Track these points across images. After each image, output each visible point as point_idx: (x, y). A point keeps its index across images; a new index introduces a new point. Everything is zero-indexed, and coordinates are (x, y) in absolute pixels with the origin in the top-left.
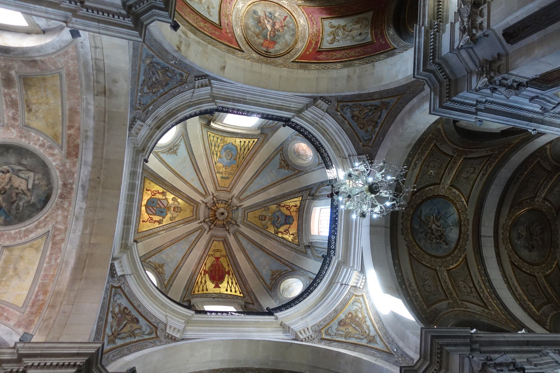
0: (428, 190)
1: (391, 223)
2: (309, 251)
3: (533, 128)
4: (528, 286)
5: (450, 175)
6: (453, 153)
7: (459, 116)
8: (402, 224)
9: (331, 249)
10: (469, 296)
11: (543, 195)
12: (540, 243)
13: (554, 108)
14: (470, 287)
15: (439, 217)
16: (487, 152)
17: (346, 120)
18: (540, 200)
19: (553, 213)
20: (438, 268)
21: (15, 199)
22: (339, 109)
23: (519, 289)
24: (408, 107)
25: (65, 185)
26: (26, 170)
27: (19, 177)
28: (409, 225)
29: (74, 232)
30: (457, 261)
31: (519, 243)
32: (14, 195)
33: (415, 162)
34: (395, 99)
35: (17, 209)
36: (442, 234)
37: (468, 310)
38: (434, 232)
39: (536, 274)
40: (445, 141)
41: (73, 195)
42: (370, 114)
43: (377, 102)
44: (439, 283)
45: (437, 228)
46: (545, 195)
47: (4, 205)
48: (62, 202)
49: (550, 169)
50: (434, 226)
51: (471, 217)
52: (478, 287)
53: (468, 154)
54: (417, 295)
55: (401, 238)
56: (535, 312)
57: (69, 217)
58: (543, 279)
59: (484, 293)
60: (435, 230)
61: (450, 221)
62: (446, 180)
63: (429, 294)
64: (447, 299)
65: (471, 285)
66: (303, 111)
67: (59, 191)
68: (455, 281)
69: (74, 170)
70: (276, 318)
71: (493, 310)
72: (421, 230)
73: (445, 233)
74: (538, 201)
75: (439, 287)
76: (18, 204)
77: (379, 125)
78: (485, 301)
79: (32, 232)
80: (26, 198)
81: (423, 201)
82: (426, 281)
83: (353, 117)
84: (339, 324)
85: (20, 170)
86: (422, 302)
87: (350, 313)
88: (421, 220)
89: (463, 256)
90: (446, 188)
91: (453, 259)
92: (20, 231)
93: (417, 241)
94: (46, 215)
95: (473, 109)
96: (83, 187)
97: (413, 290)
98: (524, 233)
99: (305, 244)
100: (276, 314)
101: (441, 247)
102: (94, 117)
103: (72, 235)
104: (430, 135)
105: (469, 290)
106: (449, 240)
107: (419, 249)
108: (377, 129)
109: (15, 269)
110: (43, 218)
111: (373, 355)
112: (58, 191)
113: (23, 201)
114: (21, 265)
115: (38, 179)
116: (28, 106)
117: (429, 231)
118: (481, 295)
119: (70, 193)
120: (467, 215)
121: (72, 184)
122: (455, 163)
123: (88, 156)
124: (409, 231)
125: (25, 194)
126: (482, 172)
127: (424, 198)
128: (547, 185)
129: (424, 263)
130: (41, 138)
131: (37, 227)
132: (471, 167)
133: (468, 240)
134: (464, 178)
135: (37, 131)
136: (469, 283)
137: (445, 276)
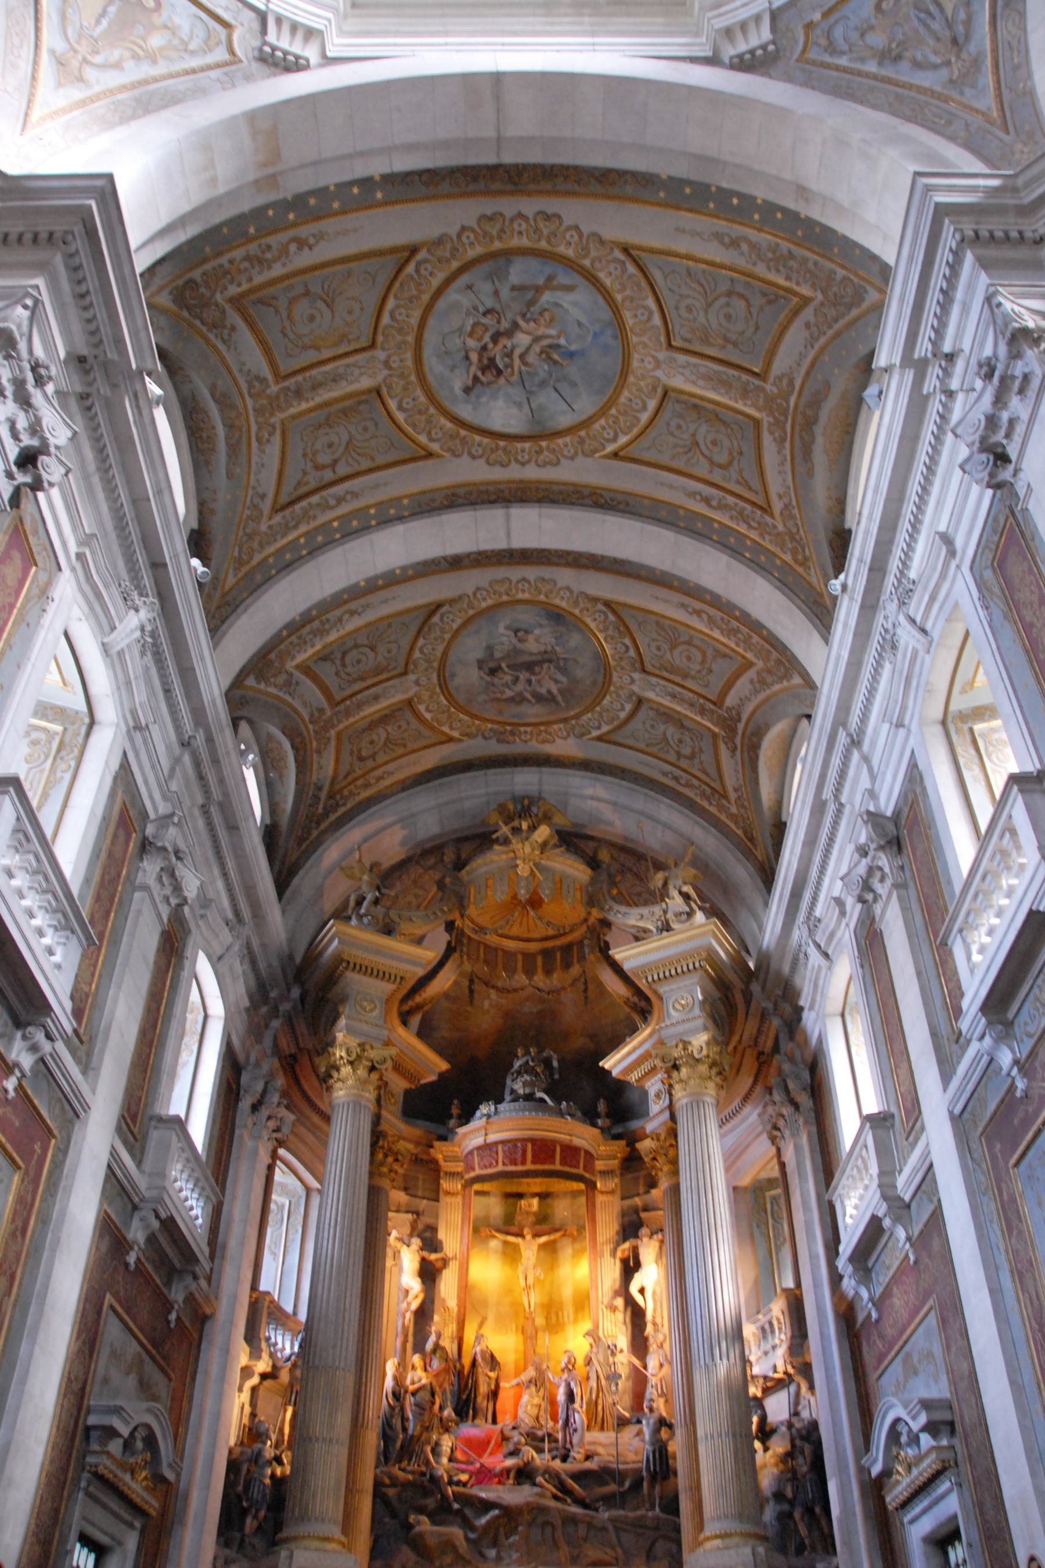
0: (646, 308)
1: (517, 166)
3: (850, 582)
4: (373, 648)
5: (701, 383)
6: (780, 378)
7: (902, 300)
8: (520, 215)
10: (305, 455)
11: (650, 695)
12: (509, 693)
13: (913, 621)
14: (335, 462)
15: (555, 357)
16: (780, 497)
18: (635, 688)
19: (599, 728)
20: (381, 355)
23: (356, 622)
28: (516, 242)
30: (414, 426)
31: (501, 629)
33: (745, 239)
36: (499, 372)
37: (254, 444)
38: (504, 341)
39: (412, 677)
40: (817, 339)
44: (326, 354)
45: (517, 352)
46: (649, 700)
49: (730, 700)
50: (522, 339)
52: (339, 489)
53: (771, 433)
54: (270, 267)
56: (293, 658)
58: (400, 697)
59: (325, 507)
60: (509, 345)
61: (546, 398)
62: (687, 372)
63: (285, 314)
65: (342, 470)
68: (344, 412)
71: (270, 527)
72: (505, 293)
73: (502, 381)
74: (633, 681)
75: (312, 356)
78: (297, 507)
81: (605, 294)
82: (328, 305)
86: (250, 279)
88: (538, 290)
89: (435, 447)
90: (659, 373)
91: (420, 412)
93: (464, 279)
95: (923, 348)
97: (284, 251)
98: (532, 646)
101: (453, 368)
104: (841, 273)
105: (324, 459)
106: (484, 399)
107: (436, 282)
117: (505, 325)
118: (315, 499)
120: (572, 458)
122: (745, 393)
124: (497, 245)
126: (714, 492)
127: (619, 297)
128: (682, 701)
129: (391, 303)
132: (730, 454)
133: (488, 463)
134: (694, 435)
136: (348, 463)
137: (357, 381)
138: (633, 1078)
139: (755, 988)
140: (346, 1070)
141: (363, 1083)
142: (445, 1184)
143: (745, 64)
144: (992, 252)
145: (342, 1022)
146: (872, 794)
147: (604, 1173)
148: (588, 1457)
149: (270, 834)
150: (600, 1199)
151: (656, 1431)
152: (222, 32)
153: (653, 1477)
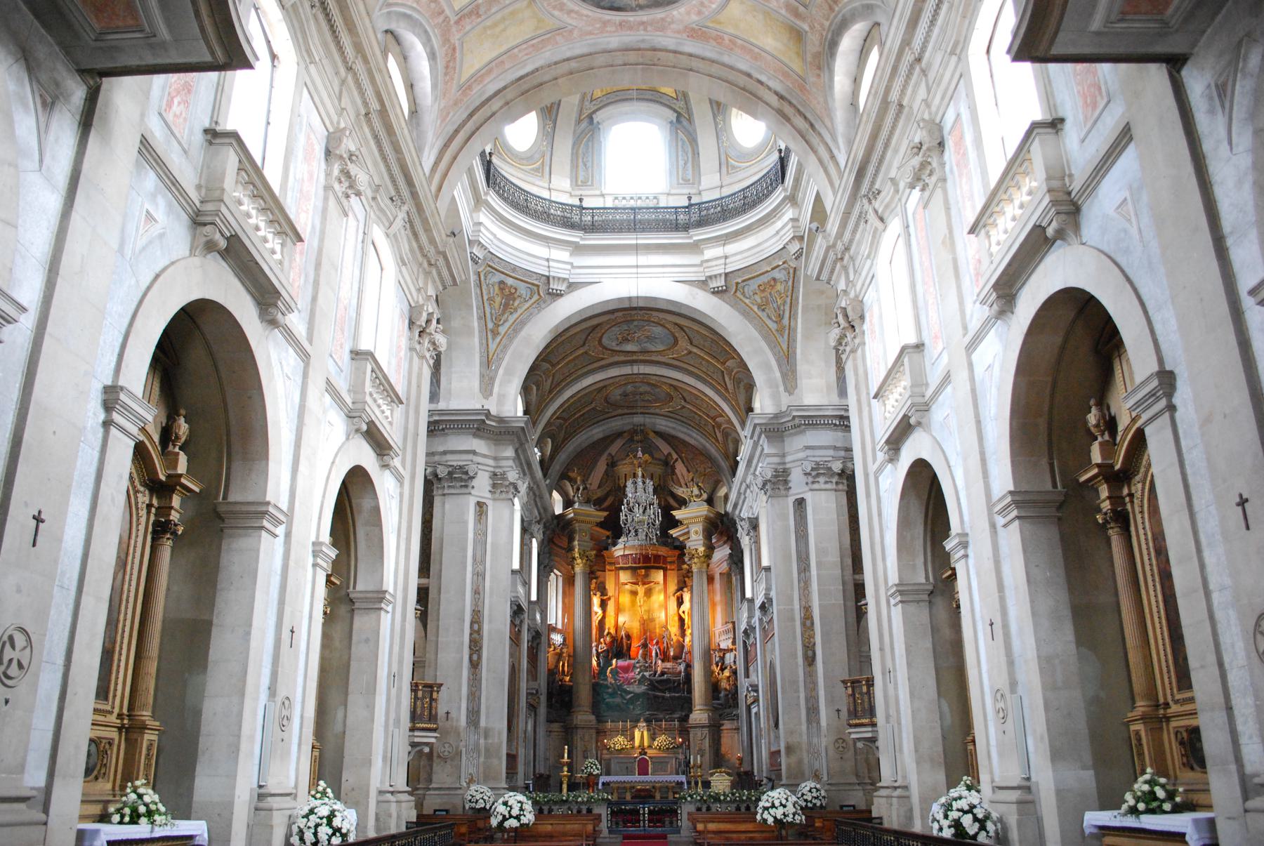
2: (584, 124)
9: (593, 225)
17: (773, 269)
22: (786, 265)
24: (774, 363)
25: (643, 23)
34: (785, 347)
42: (775, 305)
43: (786, 321)
51: (654, 358)
55: (620, 314)
64: (553, 365)
66: (792, 205)
67: (631, 19)
69: (669, 33)
70: (486, 194)
77: (760, 313)
79: (561, 10)
83: (774, 279)
84: (502, 282)
87: (516, 289)
95: (755, 438)
96: (643, 41)
99: (594, 116)
100: (491, 192)
102: (749, 75)
108: (756, 310)
109: (504, 30)
111: (481, 344)
112: (630, 17)
119: (631, 28)
123: (690, 47)
130: (714, 6)
138: (681, 539)
139: (725, 519)
140: (579, 561)
141: (585, 564)
142: (608, 567)
143: (716, 292)
144: (770, 434)
145: (576, 543)
146: (751, 507)
147: (670, 562)
148: (663, 674)
149: (542, 462)
150: (669, 572)
151: (686, 669)
152: (535, 288)
153: (684, 683)
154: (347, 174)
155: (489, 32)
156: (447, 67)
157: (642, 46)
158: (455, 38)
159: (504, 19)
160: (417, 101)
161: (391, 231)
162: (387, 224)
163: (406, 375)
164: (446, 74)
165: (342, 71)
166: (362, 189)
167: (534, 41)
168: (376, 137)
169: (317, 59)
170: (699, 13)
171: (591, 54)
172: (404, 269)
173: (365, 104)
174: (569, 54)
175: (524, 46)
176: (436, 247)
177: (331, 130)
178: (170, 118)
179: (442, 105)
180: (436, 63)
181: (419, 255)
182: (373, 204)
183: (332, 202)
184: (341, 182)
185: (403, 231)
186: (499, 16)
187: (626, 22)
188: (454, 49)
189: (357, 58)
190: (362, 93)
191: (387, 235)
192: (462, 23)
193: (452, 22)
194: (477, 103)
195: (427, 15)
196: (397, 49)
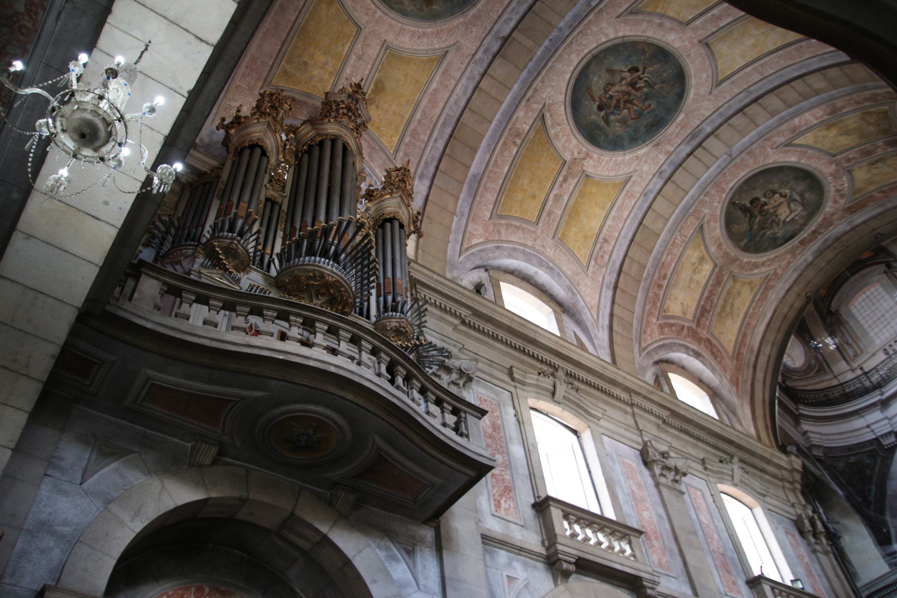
21: (767, 225)
25: (814, 232)
26: (800, 203)
27: (789, 205)
29: (785, 283)
32: (770, 221)
35: (762, 237)
41: (812, 244)
47: (755, 227)
48: (798, 247)
57: (791, 265)
67: (805, 235)
76: (766, 232)
80: (776, 229)
85: (795, 200)
92: (750, 262)
94: (777, 254)
96: (826, 240)
103: (781, 285)
109: (732, 306)
110: (773, 256)
112: (804, 235)
113: (772, 231)
114: (737, 303)
115: (800, 216)
116: (877, 161)
119: (811, 241)
121: (820, 234)
125: (778, 225)
130: (846, 185)
131: (763, 264)
135: (852, 180)
154: (669, 469)
155: (723, 315)
156: (713, 354)
157: (828, 243)
158: (704, 334)
159: (726, 301)
160: (711, 386)
161: (736, 480)
162: (730, 478)
163: (820, 572)
164: (716, 358)
165: (629, 409)
166: (684, 470)
167: (757, 297)
168: (681, 430)
169: (600, 415)
170: (842, 196)
171: (800, 275)
172: (767, 499)
173: (658, 417)
174: (787, 286)
175: (754, 304)
176: (785, 469)
177: (640, 448)
178: (502, 513)
179: (729, 377)
180: (704, 357)
181: (777, 482)
182: (708, 472)
183: (665, 492)
184: (664, 476)
185: (746, 476)
186: (721, 302)
187: (804, 240)
188: (709, 341)
189: (631, 396)
190: (651, 412)
191: (735, 485)
192: (702, 323)
193: (694, 327)
194: (753, 358)
195: (675, 336)
196: (674, 367)
